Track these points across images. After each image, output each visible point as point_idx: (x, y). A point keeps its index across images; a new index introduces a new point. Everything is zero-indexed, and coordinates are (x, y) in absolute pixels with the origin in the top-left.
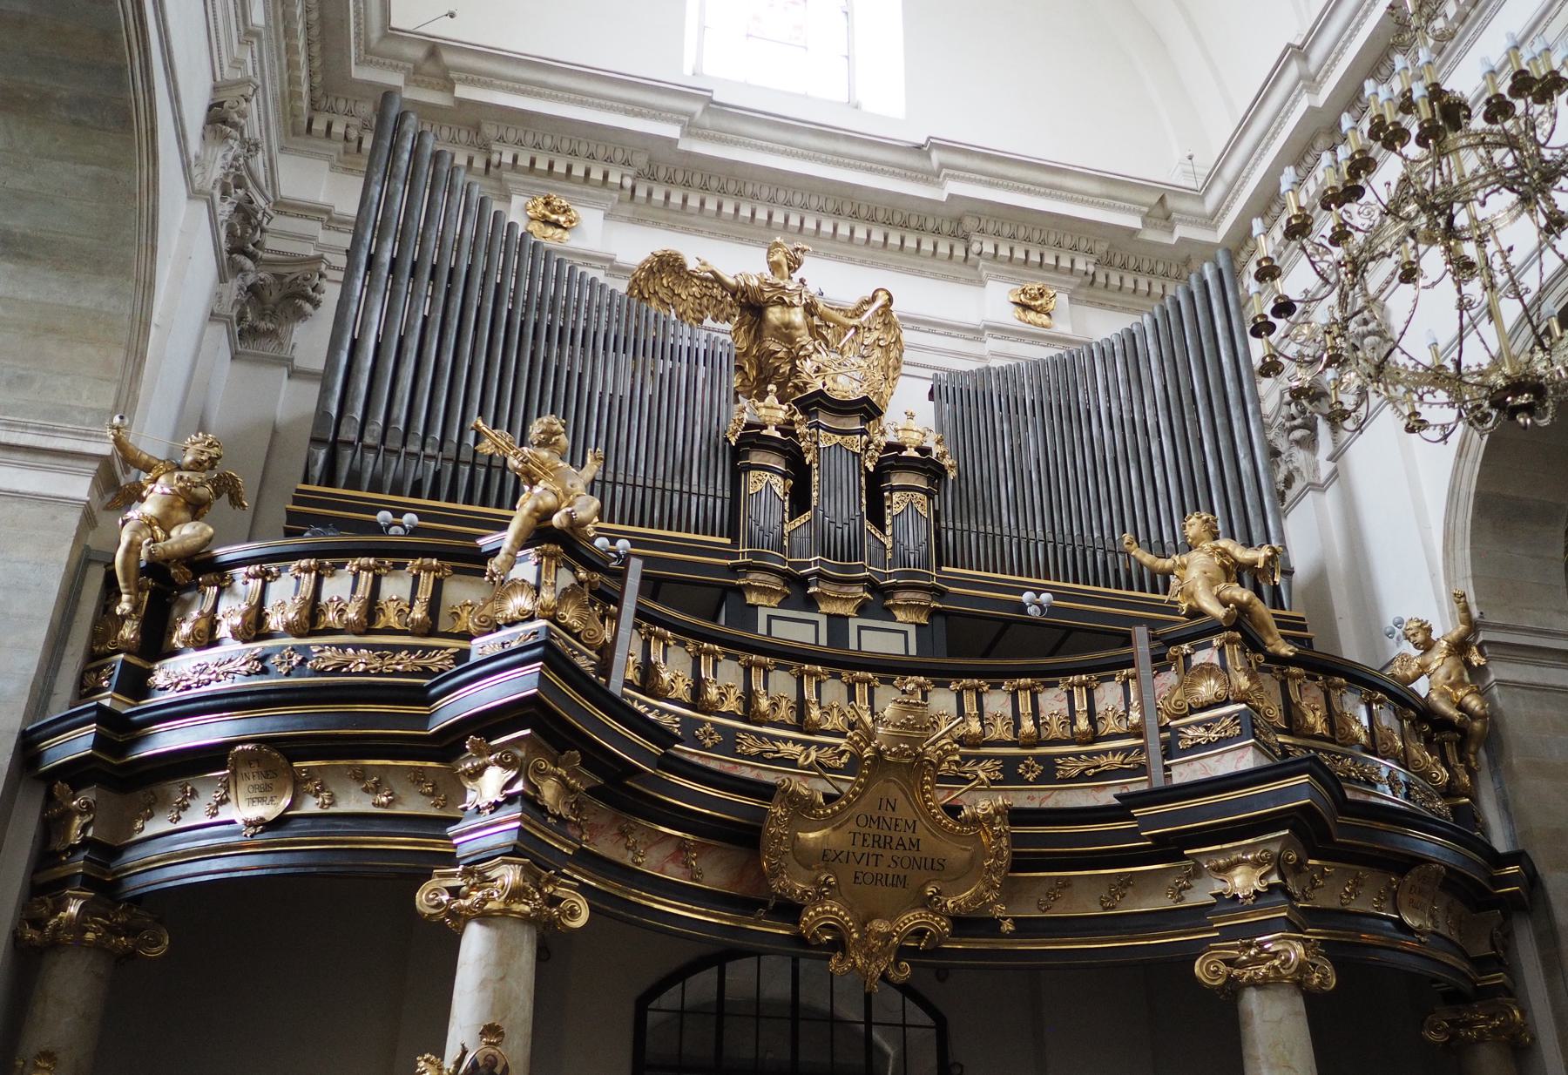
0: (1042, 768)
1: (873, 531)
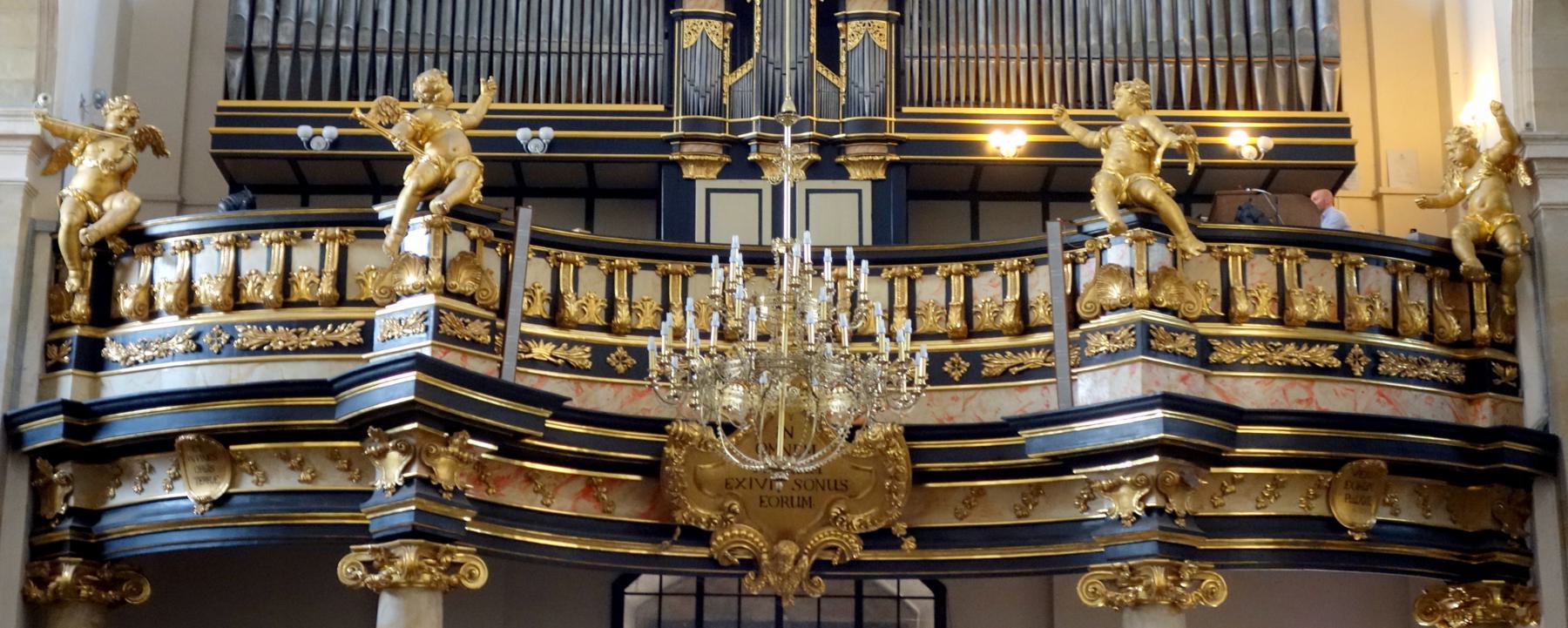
0: (968, 365)
1: (824, 73)
